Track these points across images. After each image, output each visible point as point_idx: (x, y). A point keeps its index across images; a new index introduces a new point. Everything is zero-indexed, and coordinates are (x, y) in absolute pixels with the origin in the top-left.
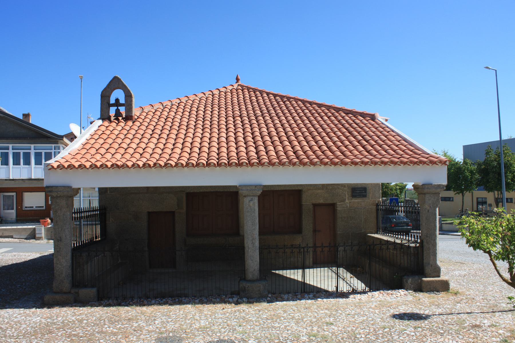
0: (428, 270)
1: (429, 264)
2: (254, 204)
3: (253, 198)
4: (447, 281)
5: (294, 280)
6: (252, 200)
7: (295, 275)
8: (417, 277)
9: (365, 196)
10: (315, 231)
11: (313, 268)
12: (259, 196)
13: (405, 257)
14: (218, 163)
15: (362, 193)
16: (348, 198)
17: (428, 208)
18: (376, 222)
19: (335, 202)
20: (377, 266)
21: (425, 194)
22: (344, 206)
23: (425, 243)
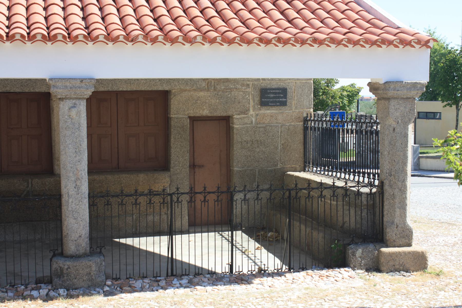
0: (390, 233)
1: (393, 223)
2: (78, 113)
3: (77, 102)
4: (423, 253)
5: (154, 254)
7: (156, 245)
8: (371, 247)
9: (284, 104)
10: (193, 166)
11: (188, 232)
12: (87, 100)
13: (352, 212)
14: (7, 34)
15: (279, 97)
16: (254, 107)
17: (394, 124)
18: (302, 150)
19: (229, 113)
20: (303, 227)
21: (388, 99)
22: (246, 120)
23: (386, 187)
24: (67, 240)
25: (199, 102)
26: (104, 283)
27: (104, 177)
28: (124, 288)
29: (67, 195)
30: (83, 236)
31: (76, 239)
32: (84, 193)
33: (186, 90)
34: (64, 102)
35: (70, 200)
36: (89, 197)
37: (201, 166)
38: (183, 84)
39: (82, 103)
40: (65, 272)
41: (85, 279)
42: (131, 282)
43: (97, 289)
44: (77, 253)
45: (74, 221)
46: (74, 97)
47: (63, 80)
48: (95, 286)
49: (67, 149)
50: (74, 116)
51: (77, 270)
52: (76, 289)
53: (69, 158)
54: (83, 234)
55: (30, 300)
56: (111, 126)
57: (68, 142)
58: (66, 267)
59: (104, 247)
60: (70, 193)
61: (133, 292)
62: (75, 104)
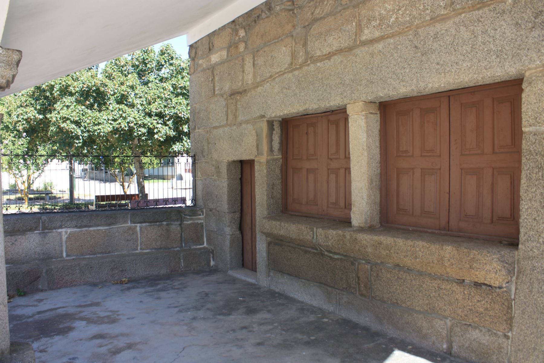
27: (392, 240)
56: (440, 156)
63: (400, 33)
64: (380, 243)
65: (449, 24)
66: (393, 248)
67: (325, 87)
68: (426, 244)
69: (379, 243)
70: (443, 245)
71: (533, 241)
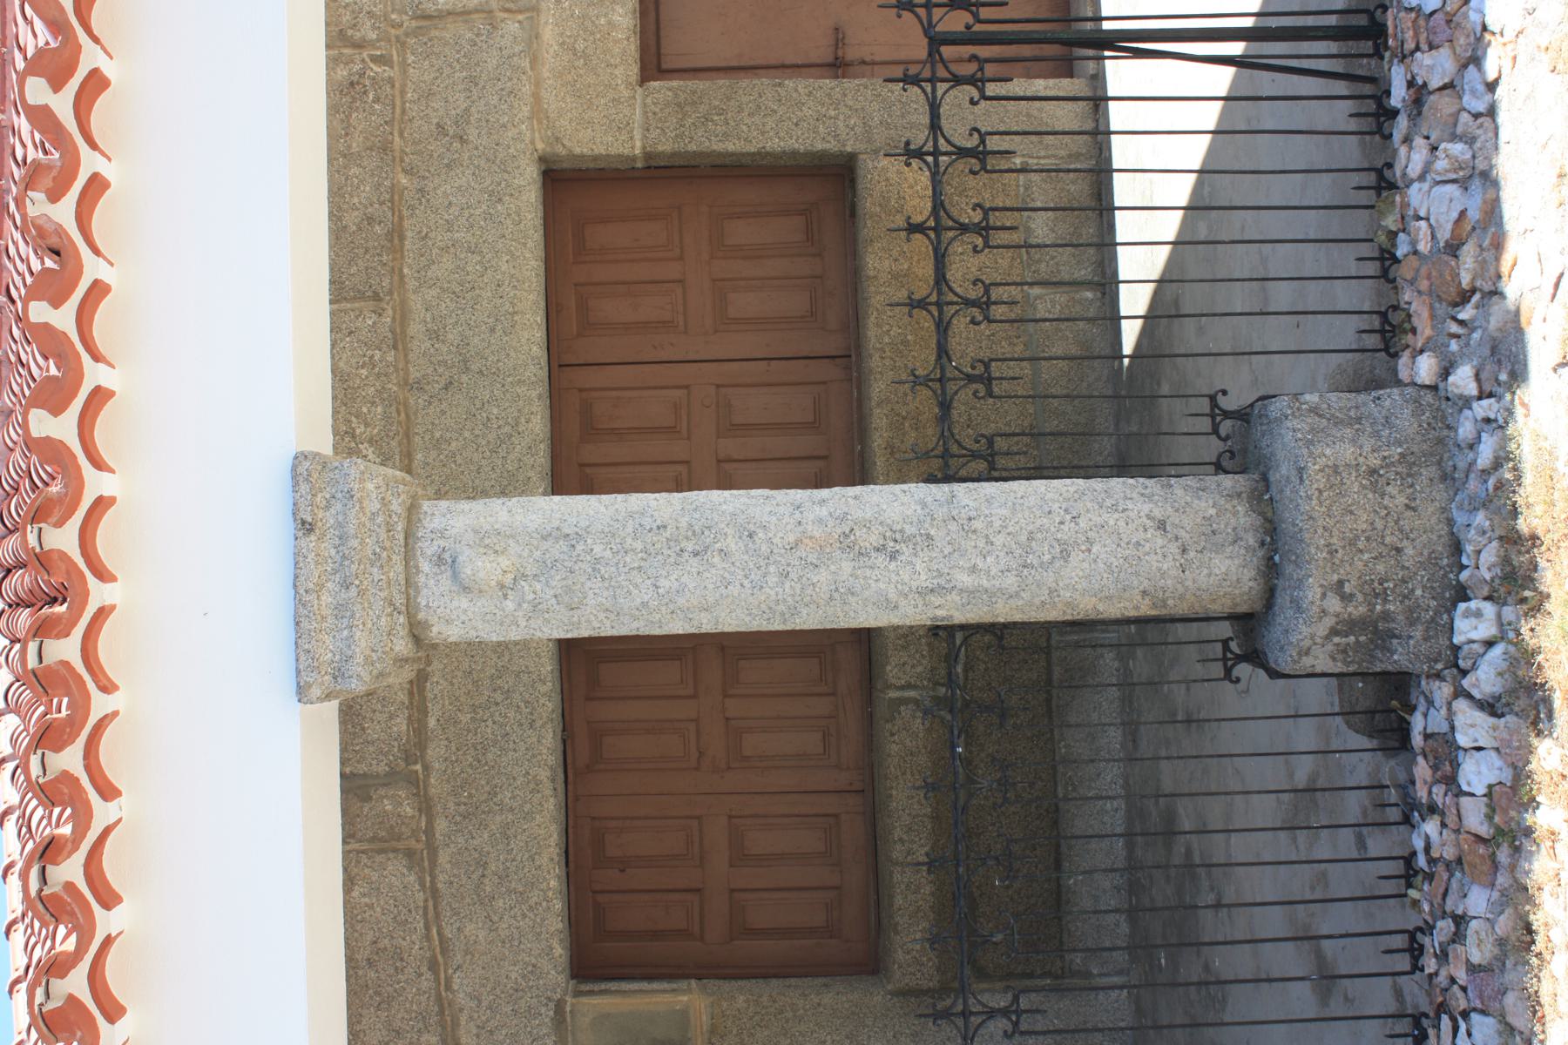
2: (487, 541)
6: (446, 562)
10: (838, 66)
24: (1182, 597)
25: (580, 45)
26: (1428, 397)
28: (1466, 279)
29: (936, 600)
30: (1157, 513)
31: (1174, 548)
32: (924, 505)
33: (536, 97)
34: (433, 620)
35: (964, 579)
36: (948, 479)
37: (839, 36)
38: (511, 107)
39: (437, 523)
40: (1362, 609)
41: (1401, 500)
42: (1424, 247)
43: (1466, 430)
44: (1251, 541)
45: (1076, 557)
46: (400, 568)
47: (305, 624)
48: (1440, 441)
49: (681, 601)
50: (505, 562)
51: (1352, 543)
52: (1457, 548)
53: (734, 590)
54: (1146, 508)
55: (1533, 804)
56: (687, 387)
57: (646, 594)
58: (1334, 604)
59: (1213, 398)
60: (924, 580)
61: (1500, 224)
62: (439, 561)
63: (407, 435)
64: (891, 449)
65: (416, 303)
66: (896, 407)
67: (498, 697)
68: (872, 319)
69: (892, 453)
70: (869, 277)
71: (837, 127)
